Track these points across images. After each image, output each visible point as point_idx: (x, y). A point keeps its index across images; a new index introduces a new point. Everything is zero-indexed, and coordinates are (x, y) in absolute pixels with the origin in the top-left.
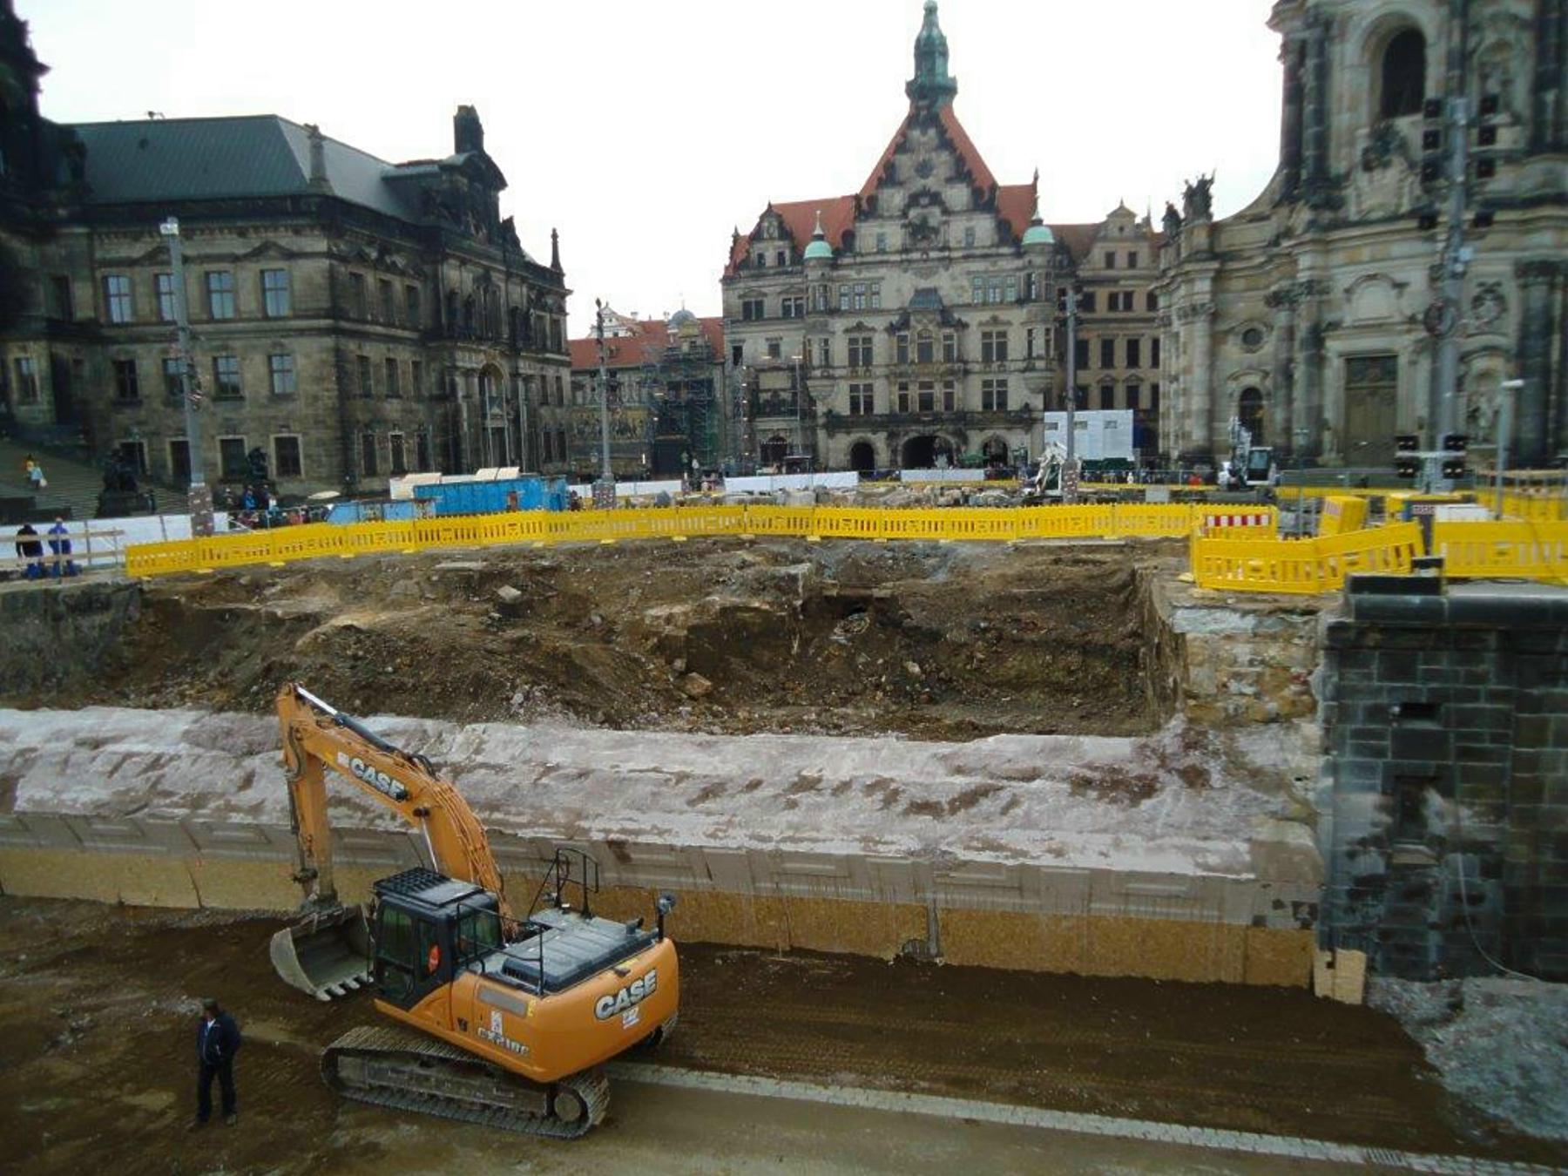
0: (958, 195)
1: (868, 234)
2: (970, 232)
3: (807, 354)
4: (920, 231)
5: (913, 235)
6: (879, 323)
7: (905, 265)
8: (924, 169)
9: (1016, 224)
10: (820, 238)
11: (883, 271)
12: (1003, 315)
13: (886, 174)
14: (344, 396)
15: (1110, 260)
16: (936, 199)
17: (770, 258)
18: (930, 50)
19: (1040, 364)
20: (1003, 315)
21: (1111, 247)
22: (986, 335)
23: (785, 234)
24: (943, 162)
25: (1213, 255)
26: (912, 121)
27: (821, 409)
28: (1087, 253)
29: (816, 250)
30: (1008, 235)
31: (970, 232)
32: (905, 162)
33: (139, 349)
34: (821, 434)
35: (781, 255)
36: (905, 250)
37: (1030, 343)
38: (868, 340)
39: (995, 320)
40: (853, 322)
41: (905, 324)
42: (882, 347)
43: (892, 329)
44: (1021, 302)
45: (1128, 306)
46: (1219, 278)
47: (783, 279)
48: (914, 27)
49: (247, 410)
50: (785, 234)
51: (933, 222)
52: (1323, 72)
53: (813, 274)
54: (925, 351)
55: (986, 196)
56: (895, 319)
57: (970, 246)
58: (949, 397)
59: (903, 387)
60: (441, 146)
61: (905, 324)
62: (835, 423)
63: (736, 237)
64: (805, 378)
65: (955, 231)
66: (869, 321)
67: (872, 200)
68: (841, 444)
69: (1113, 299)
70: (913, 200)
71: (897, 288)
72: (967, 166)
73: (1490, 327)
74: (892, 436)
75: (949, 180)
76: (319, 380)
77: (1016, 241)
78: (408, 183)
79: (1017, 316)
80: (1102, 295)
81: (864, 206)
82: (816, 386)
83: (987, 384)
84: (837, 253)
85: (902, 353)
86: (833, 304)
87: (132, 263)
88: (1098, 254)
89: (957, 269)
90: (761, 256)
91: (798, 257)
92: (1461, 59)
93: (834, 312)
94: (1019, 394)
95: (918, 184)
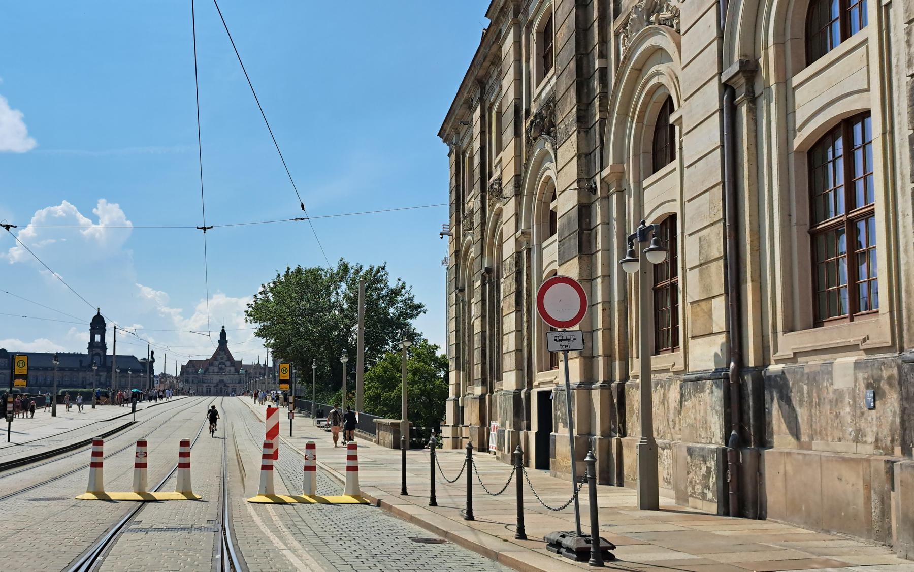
1: (211, 369)
8: (222, 358)
18: (223, 334)
24: (225, 357)
30: (237, 371)
42: (212, 388)
61: (217, 385)
65: (228, 369)
71: (216, 379)
81: (209, 363)
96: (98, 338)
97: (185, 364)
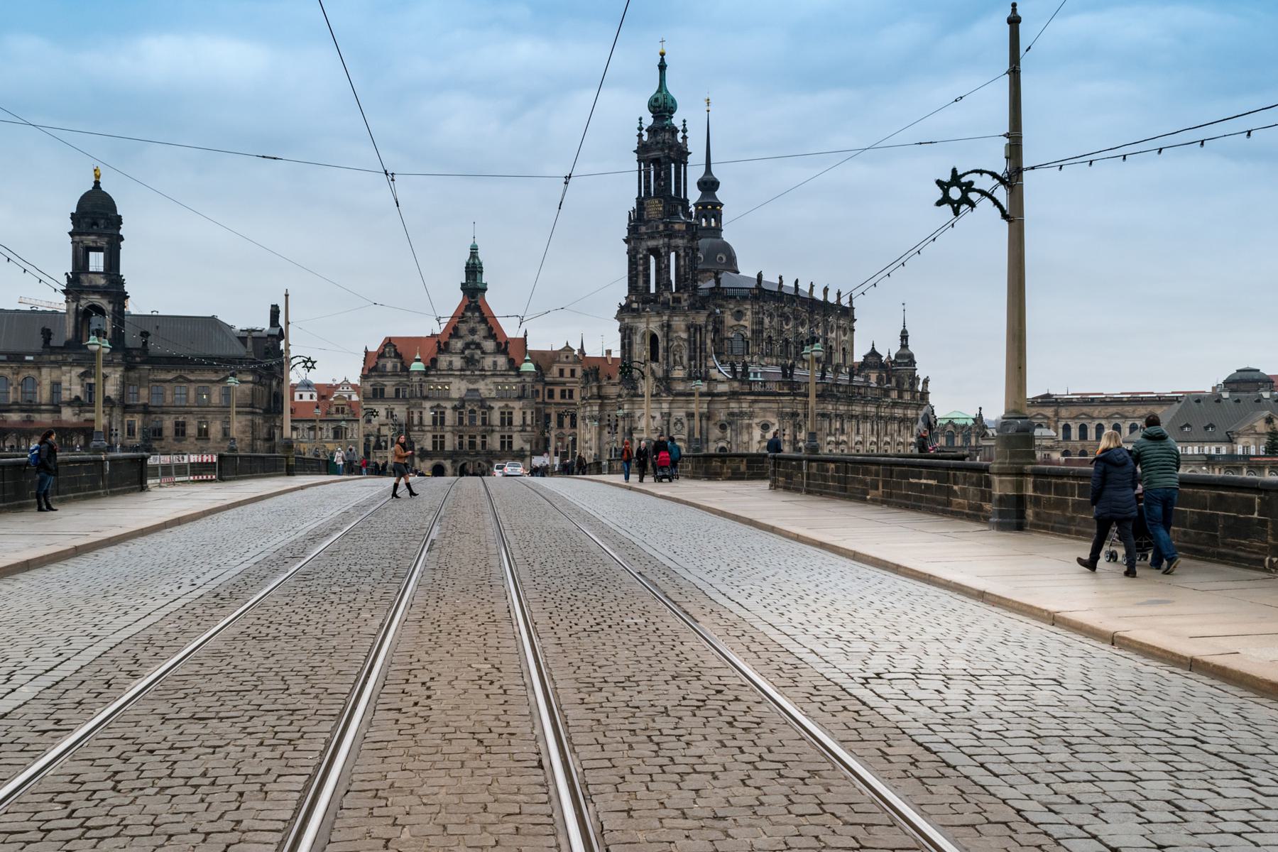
0: (489, 345)
1: (443, 360)
2: (495, 363)
3: (410, 418)
4: (470, 362)
5: (467, 362)
6: (448, 405)
7: (462, 377)
8: (473, 331)
9: (517, 361)
10: (418, 360)
11: (451, 379)
12: (511, 404)
13: (454, 332)
14: (254, 439)
15: (561, 372)
16: (478, 346)
17: (389, 366)
18: (473, 269)
19: (529, 429)
20: (511, 404)
21: (562, 366)
22: (502, 413)
23: (398, 355)
24: (482, 330)
25: (600, 397)
26: (468, 308)
27: (417, 447)
28: (550, 368)
29: (417, 366)
30: (513, 366)
31: (495, 363)
32: (464, 328)
33: (166, 417)
34: (417, 460)
35: (395, 366)
36: (462, 370)
37: (524, 419)
38: (443, 413)
39: (507, 406)
40: (435, 403)
41: (463, 406)
42: (450, 417)
43: (455, 408)
44: (519, 398)
45: (571, 397)
46: (602, 406)
47: (397, 379)
48: (466, 256)
49: (211, 444)
50: (398, 355)
51: (477, 357)
52: (630, 344)
53: (416, 379)
54: (472, 419)
55: (503, 346)
56: (456, 403)
57: (495, 369)
58: (484, 443)
59: (461, 437)
60: (264, 324)
62: (424, 455)
63: (366, 352)
64: (408, 431)
65: (488, 362)
66: (443, 404)
67: (447, 344)
68: (427, 465)
69: (563, 392)
70: (467, 346)
71: (458, 388)
72: (493, 332)
73: (679, 432)
74: (454, 462)
75: (485, 338)
76: (244, 432)
77: (518, 369)
78: (247, 337)
79: (517, 405)
80: (557, 390)
81: (442, 345)
82: (414, 435)
83: (503, 437)
84: (427, 368)
85: (461, 420)
86: (425, 393)
87: (169, 381)
88: (555, 370)
89: (488, 381)
90: (384, 366)
91: (406, 368)
92: (667, 350)
93: (426, 398)
94: (518, 443)
95: (470, 338)
96: (97, 261)
97: (374, 347)
